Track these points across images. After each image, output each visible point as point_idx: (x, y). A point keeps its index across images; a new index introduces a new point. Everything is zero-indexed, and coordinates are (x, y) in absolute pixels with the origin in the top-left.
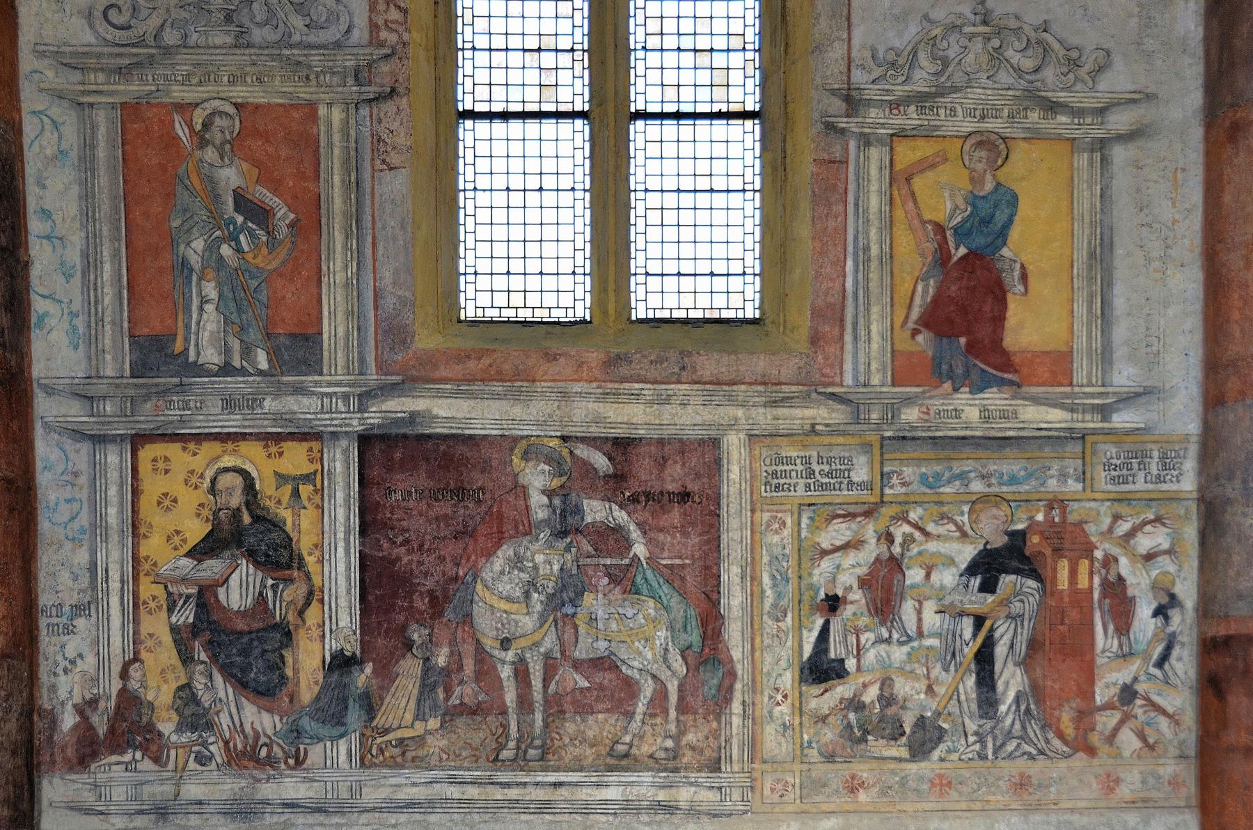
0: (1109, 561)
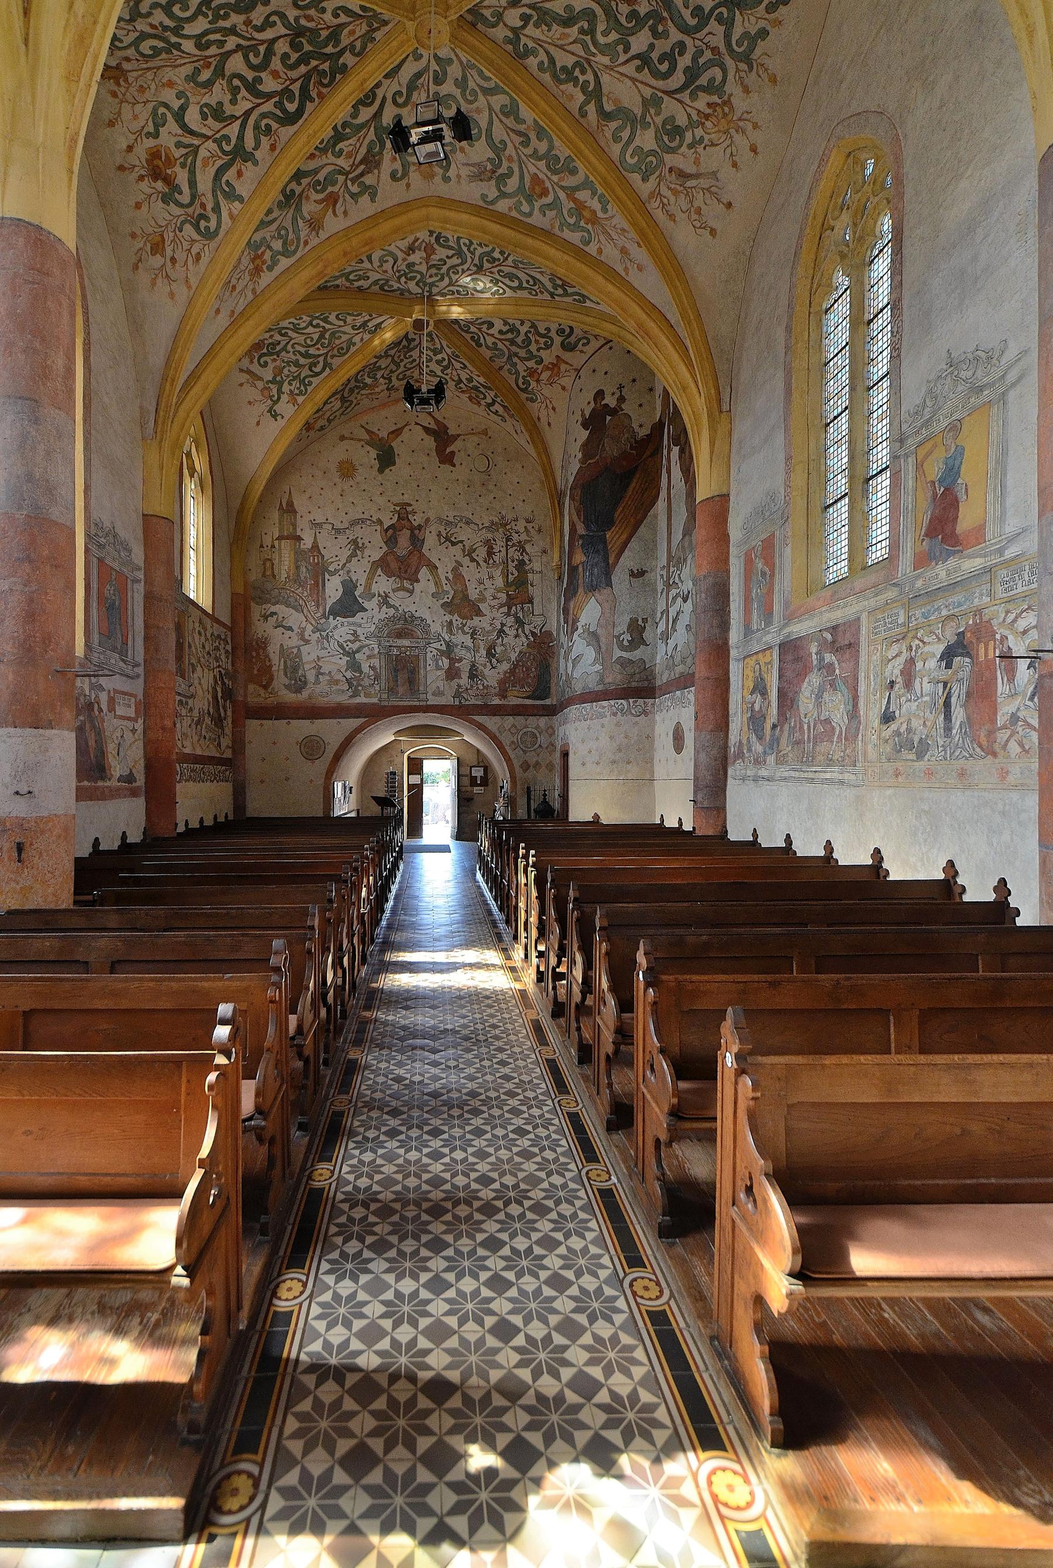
0: (1004, 638)
